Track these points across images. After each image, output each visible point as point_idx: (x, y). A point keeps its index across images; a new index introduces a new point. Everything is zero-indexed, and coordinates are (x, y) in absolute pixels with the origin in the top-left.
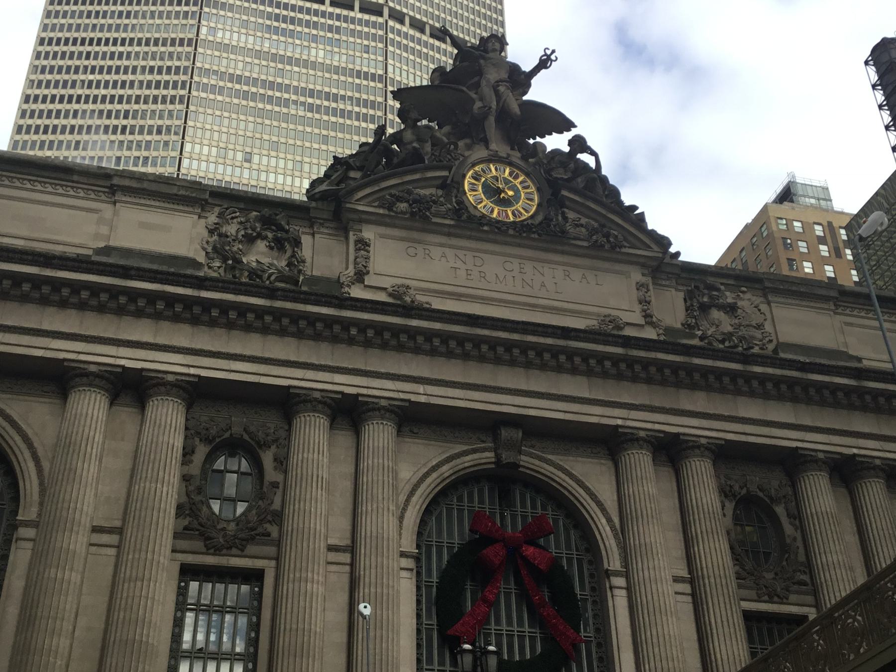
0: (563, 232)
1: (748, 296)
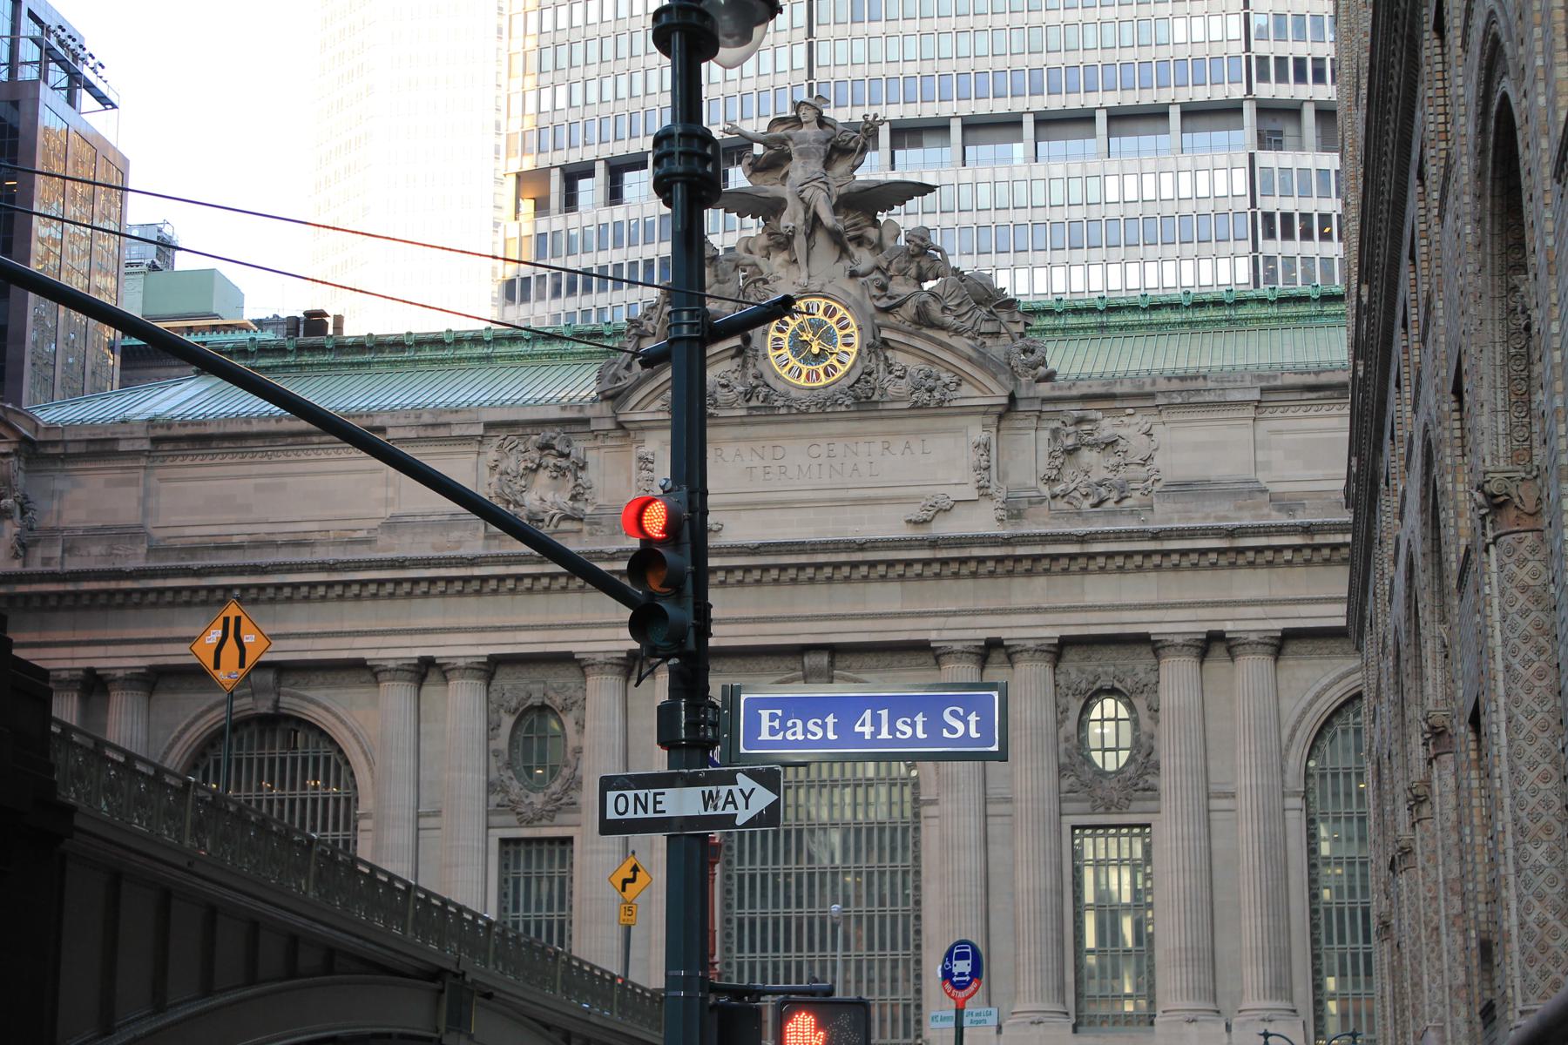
1: (1137, 418)
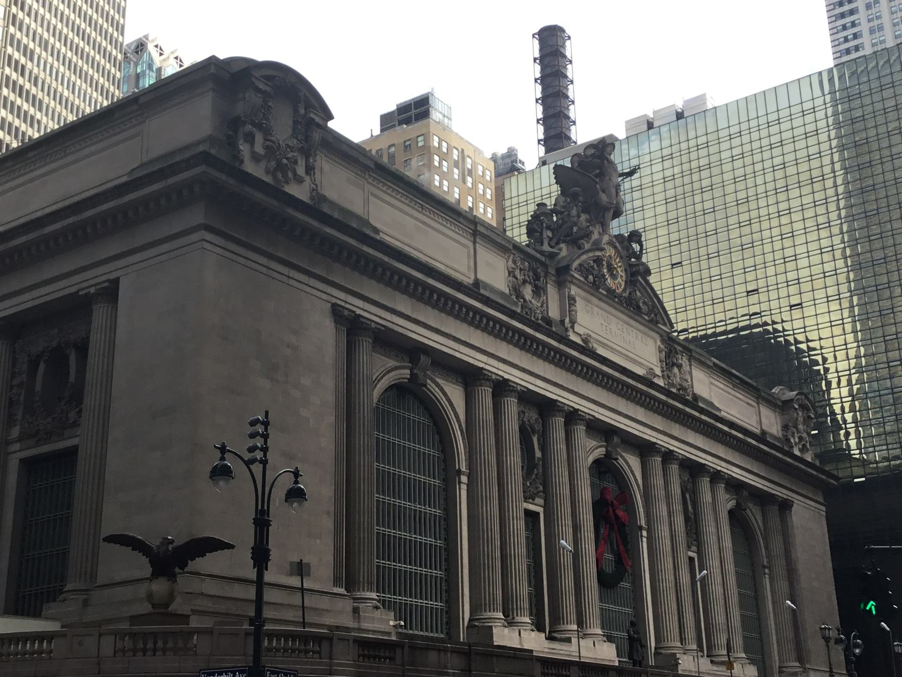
0: (639, 307)
